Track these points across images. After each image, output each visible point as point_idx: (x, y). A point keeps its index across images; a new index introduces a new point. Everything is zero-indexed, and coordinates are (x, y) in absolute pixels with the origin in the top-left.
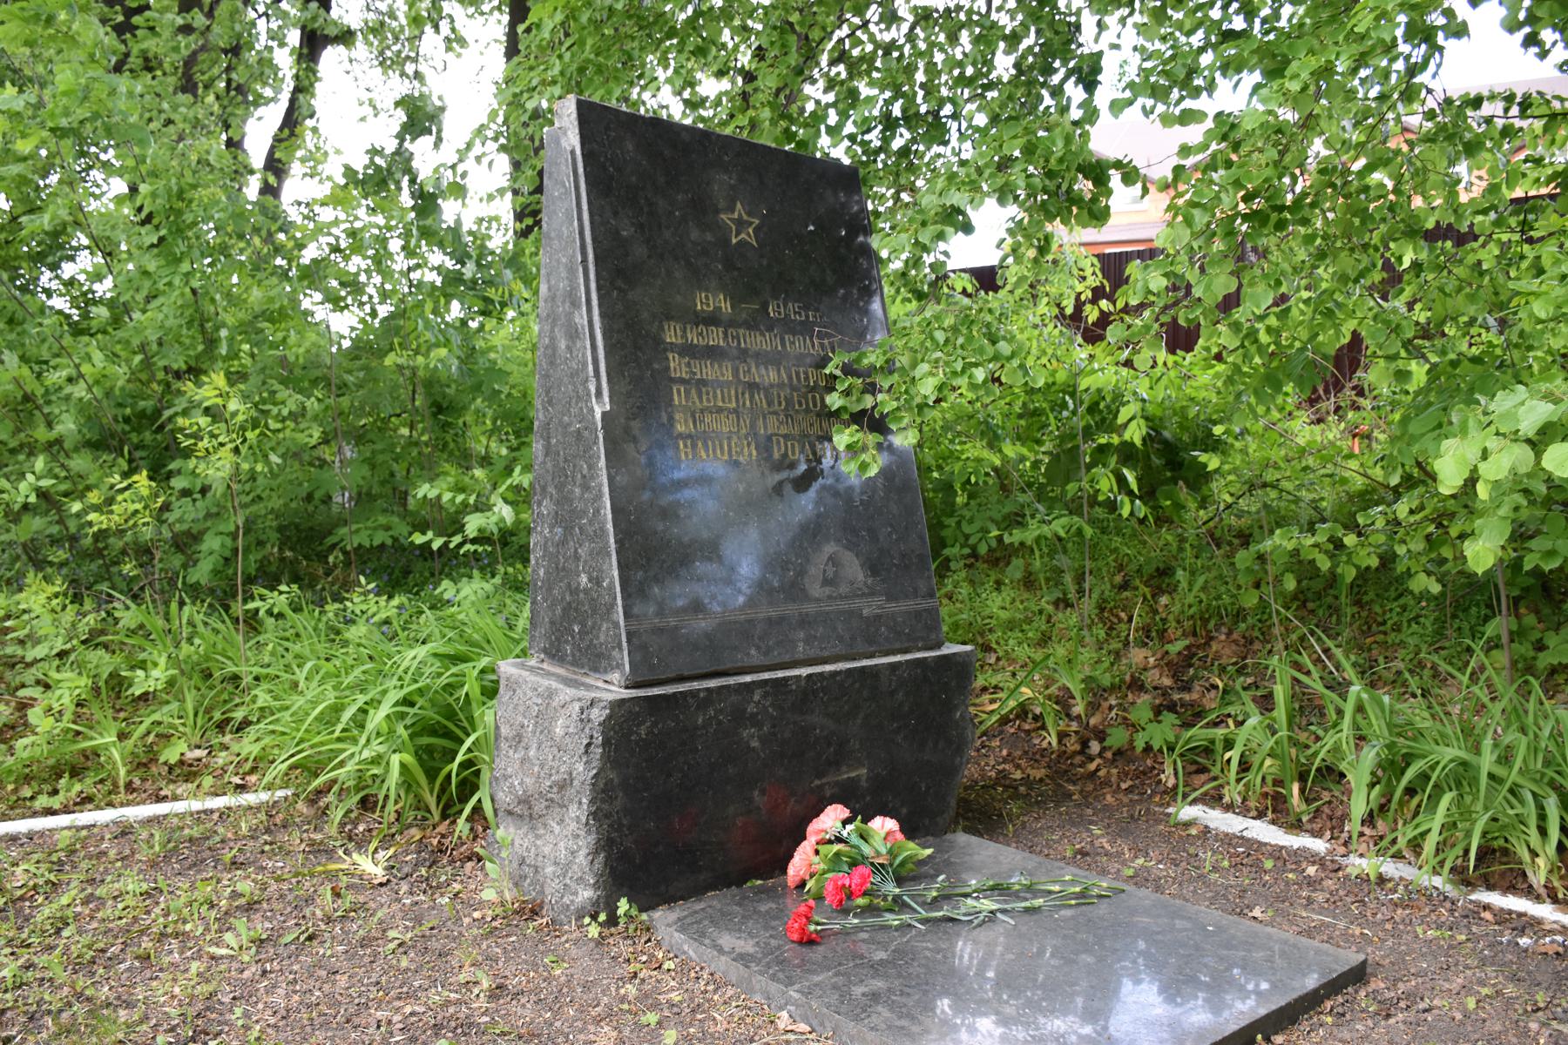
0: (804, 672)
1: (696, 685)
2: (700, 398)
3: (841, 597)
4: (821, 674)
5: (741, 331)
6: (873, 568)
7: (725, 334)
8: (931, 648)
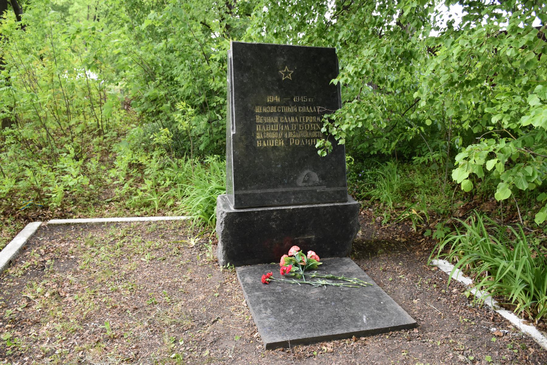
0: (292, 207)
1: (255, 210)
2: (266, 128)
3: (309, 186)
4: (298, 209)
5: (282, 107)
6: (322, 177)
7: (277, 108)
8: (343, 202)
